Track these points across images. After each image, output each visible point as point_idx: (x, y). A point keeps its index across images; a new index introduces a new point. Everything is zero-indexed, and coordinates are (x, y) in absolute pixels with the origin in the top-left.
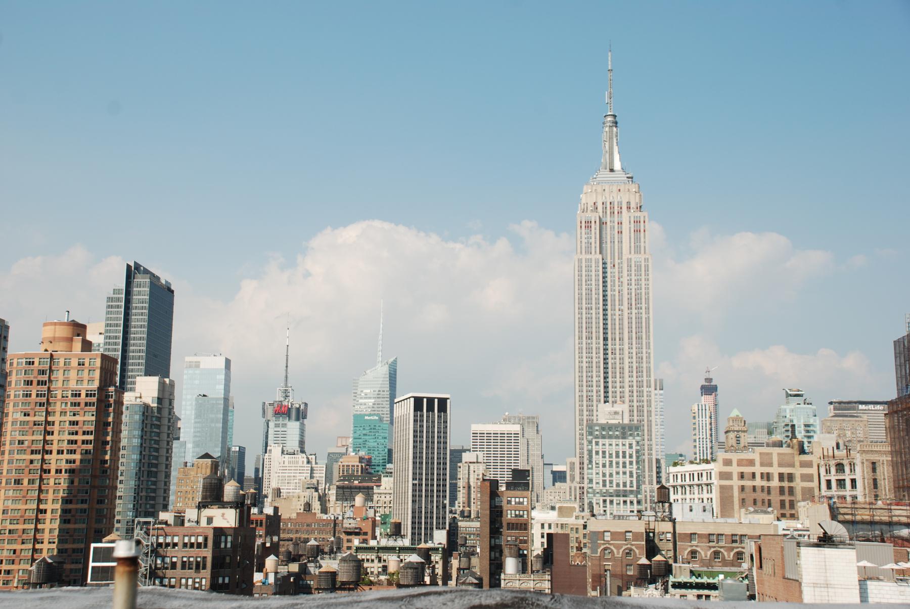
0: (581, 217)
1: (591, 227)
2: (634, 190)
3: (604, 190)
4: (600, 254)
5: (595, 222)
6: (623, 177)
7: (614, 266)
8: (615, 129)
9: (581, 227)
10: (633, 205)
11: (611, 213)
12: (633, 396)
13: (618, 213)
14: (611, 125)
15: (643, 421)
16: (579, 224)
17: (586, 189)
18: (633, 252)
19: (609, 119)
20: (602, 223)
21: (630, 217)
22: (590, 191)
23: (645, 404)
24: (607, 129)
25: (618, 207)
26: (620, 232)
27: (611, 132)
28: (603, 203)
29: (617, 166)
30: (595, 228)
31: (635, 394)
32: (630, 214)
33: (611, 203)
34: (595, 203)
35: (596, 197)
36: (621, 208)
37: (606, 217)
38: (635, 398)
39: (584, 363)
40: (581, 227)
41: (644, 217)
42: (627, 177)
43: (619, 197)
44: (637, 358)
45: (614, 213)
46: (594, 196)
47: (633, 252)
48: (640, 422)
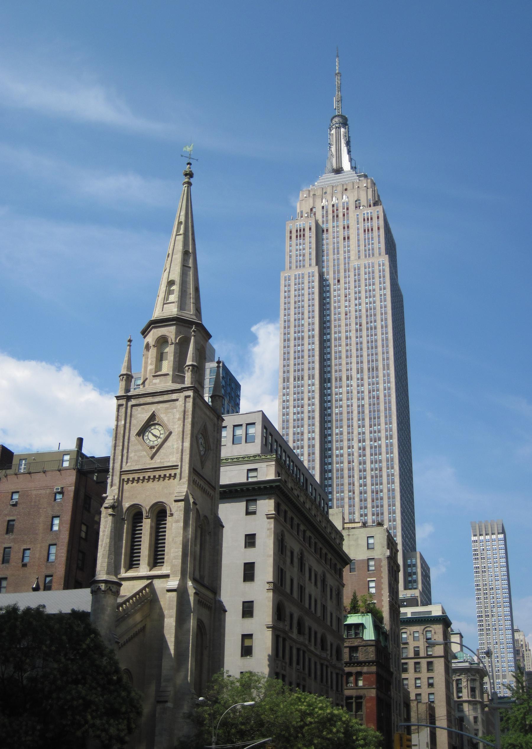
0: (292, 225)
1: (304, 235)
2: (365, 185)
3: (326, 193)
4: (317, 264)
5: (310, 229)
6: (354, 176)
7: (339, 281)
8: (342, 130)
9: (291, 238)
10: (363, 202)
11: (334, 216)
12: (364, 455)
13: (344, 215)
14: (337, 125)
15: (381, 491)
16: (288, 235)
17: (303, 195)
18: (363, 256)
19: (337, 120)
20: (320, 231)
21: (357, 215)
22: (305, 196)
23: (384, 464)
24: (333, 132)
25: (344, 208)
26: (347, 238)
27: (338, 134)
28: (323, 207)
29: (346, 165)
30: (310, 237)
31: (368, 451)
32: (358, 212)
33: (333, 206)
34: (311, 210)
35: (314, 202)
36: (348, 209)
37: (327, 222)
38: (368, 458)
39: (291, 415)
40: (291, 238)
41: (378, 212)
42: (357, 176)
43: (344, 197)
44: (370, 398)
45: (337, 216)
46: (311, 200)
47: (363, 256)
48: (377, 493)
